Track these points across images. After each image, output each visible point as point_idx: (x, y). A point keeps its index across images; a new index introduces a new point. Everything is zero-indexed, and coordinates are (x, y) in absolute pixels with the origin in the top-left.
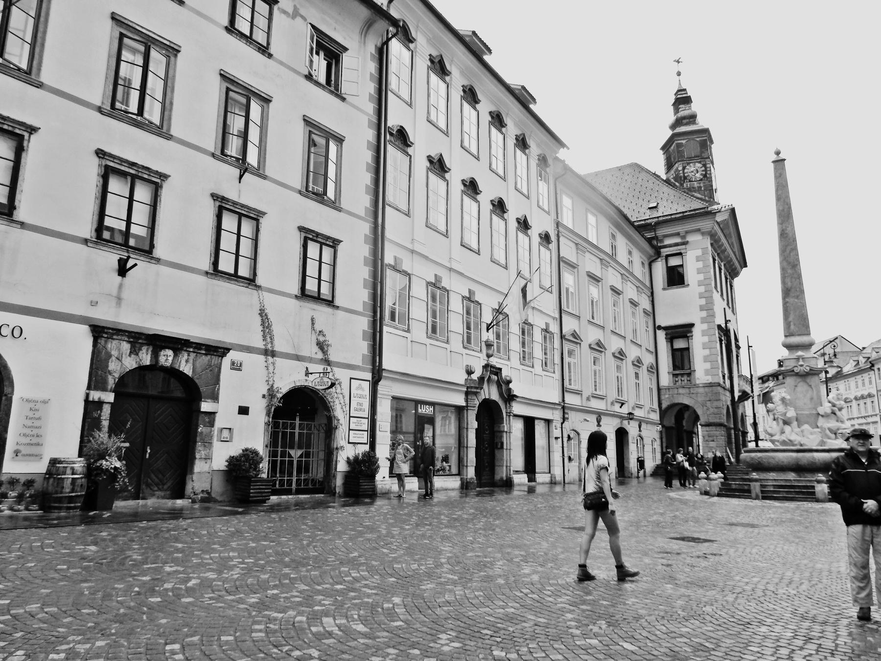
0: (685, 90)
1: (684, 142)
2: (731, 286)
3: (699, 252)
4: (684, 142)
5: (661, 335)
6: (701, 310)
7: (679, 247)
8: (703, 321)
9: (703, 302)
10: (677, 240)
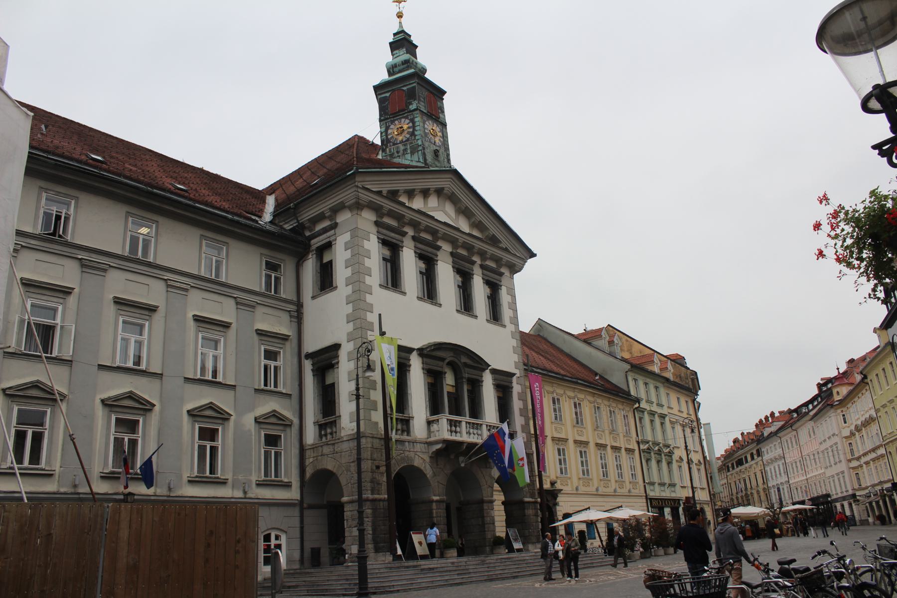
0: (403, 32)
1: (388, 95)
2: (494, 288)
3: (347, 237)
4: (388, 95)
5: (308, 365)
7: (328, 234)
9: (349, 309)
10: (326, 224)
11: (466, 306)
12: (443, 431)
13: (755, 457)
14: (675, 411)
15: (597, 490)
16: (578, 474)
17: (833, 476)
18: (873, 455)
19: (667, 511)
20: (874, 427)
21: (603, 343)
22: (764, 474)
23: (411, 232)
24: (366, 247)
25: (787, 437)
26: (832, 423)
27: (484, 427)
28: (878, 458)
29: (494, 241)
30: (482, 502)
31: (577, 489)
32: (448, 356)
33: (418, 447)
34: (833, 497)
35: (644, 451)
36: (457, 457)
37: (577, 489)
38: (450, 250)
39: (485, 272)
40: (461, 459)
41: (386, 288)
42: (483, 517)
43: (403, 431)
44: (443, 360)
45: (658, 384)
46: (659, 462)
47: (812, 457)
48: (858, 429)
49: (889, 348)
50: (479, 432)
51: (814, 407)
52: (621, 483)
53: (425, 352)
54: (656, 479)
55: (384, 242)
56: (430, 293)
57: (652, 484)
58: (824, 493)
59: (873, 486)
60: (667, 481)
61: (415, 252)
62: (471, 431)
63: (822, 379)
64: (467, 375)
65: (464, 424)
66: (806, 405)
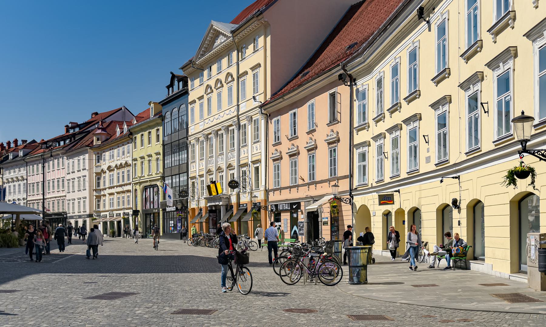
18: (120, 189)
28: (123, 192)
34: (71, 214)
47: (56, 183)
58: (61, 211)
59: (113, 211)
63: (71, 123)
66: (57, 140)
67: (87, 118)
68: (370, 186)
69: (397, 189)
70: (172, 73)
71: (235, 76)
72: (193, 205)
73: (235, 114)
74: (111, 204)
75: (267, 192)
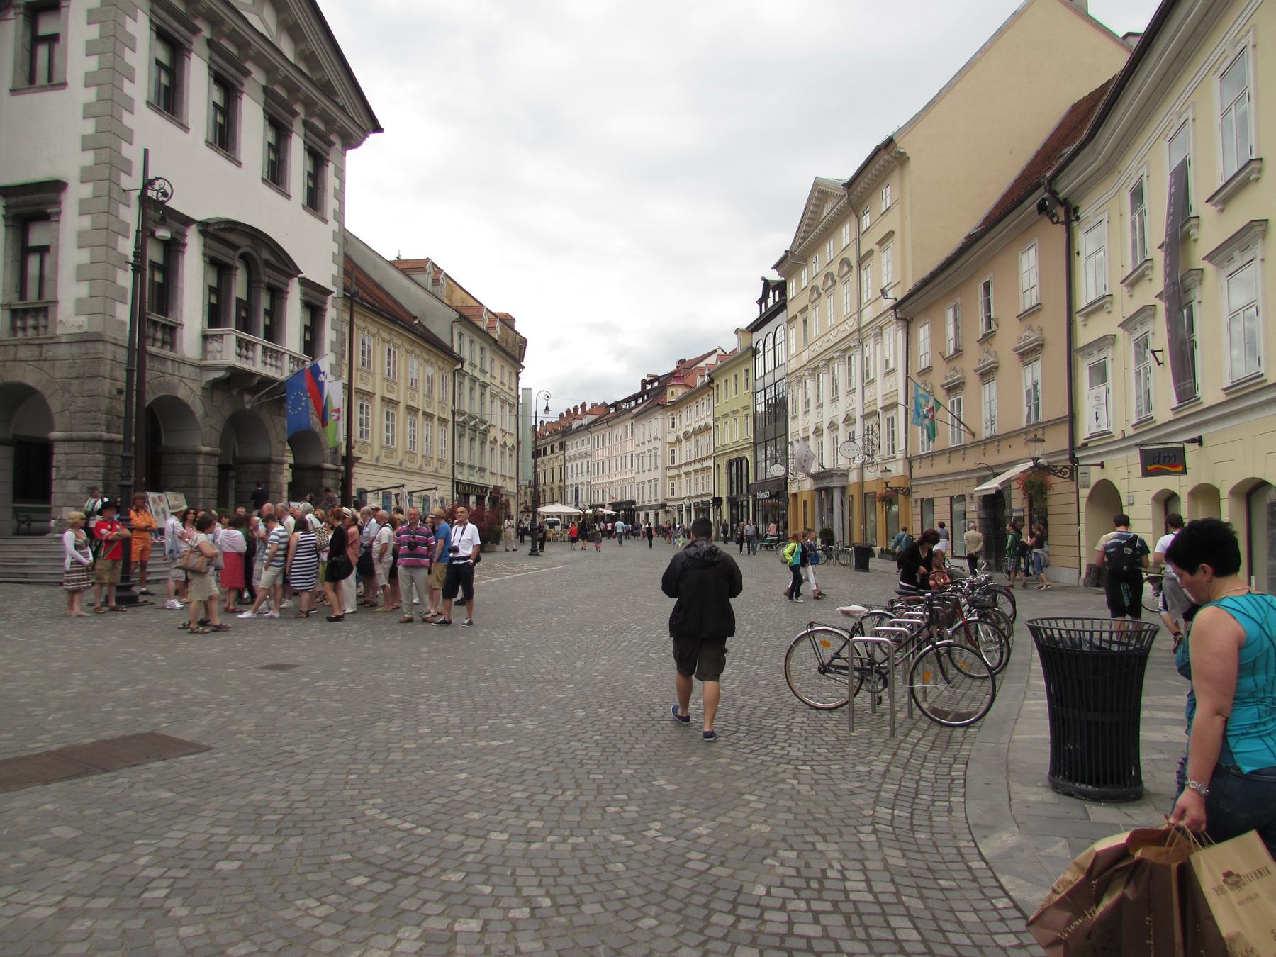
2: (317, 159)
6: (83, 150)
8: (86, 176)
9: (89, 127)
11: (276, 175)
12: (227, 352)
13: (556, 450)
14: (497, 382)
15: (401, 464)
16: (381, 441)
17: (643, 483)
18: (698, 466)
19: (473, 499)
20: (706, 438)
21: (425, 279)
22: (563, 471)
23: (206, 33)
24: (128, 29)
25: (600, 434)
26: (656, 425)
27: (287, 357)
28: (702, 470)
29: (327, 89)
30: (268, 461)
31: (377, 459)
32: (245, 244)
33: (186, 371)
35: (459, 424)
36: (241, 394)
37: (377, 459)
38: (263, 82)
39: (309, 134)
40: (247, 397)
41: (157, 110)
42: (268, 482)
43: (164, 343)
44: (235, 247)
45: (486, 346)
46: (472, 439)
48: (687, 436)
49: (750, 353)
50: (279, 364)
51: (637, 406)
52: (428, 459)
53: (211, 229)
54: (466, 461)
55: (162, 34)
56: (224, 137)
57: (461, 465)
59: (689, 498)
60: (477, 464)
61: (209, 67)
62: (268, 360)
64: (267, 279)
65: (259, 349)
66: (628, 401)
67: (672, 367)
68: (1119, 436)
69: (1194, 435)
70: (764, 279)
71: (854, 263)
72: (792, 489)
73: (856, 327)
74: (688, 486)
75: (909, 460)
